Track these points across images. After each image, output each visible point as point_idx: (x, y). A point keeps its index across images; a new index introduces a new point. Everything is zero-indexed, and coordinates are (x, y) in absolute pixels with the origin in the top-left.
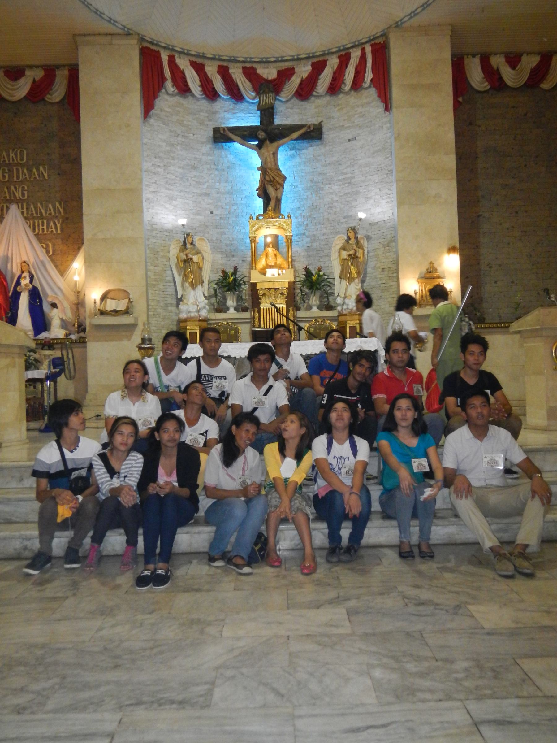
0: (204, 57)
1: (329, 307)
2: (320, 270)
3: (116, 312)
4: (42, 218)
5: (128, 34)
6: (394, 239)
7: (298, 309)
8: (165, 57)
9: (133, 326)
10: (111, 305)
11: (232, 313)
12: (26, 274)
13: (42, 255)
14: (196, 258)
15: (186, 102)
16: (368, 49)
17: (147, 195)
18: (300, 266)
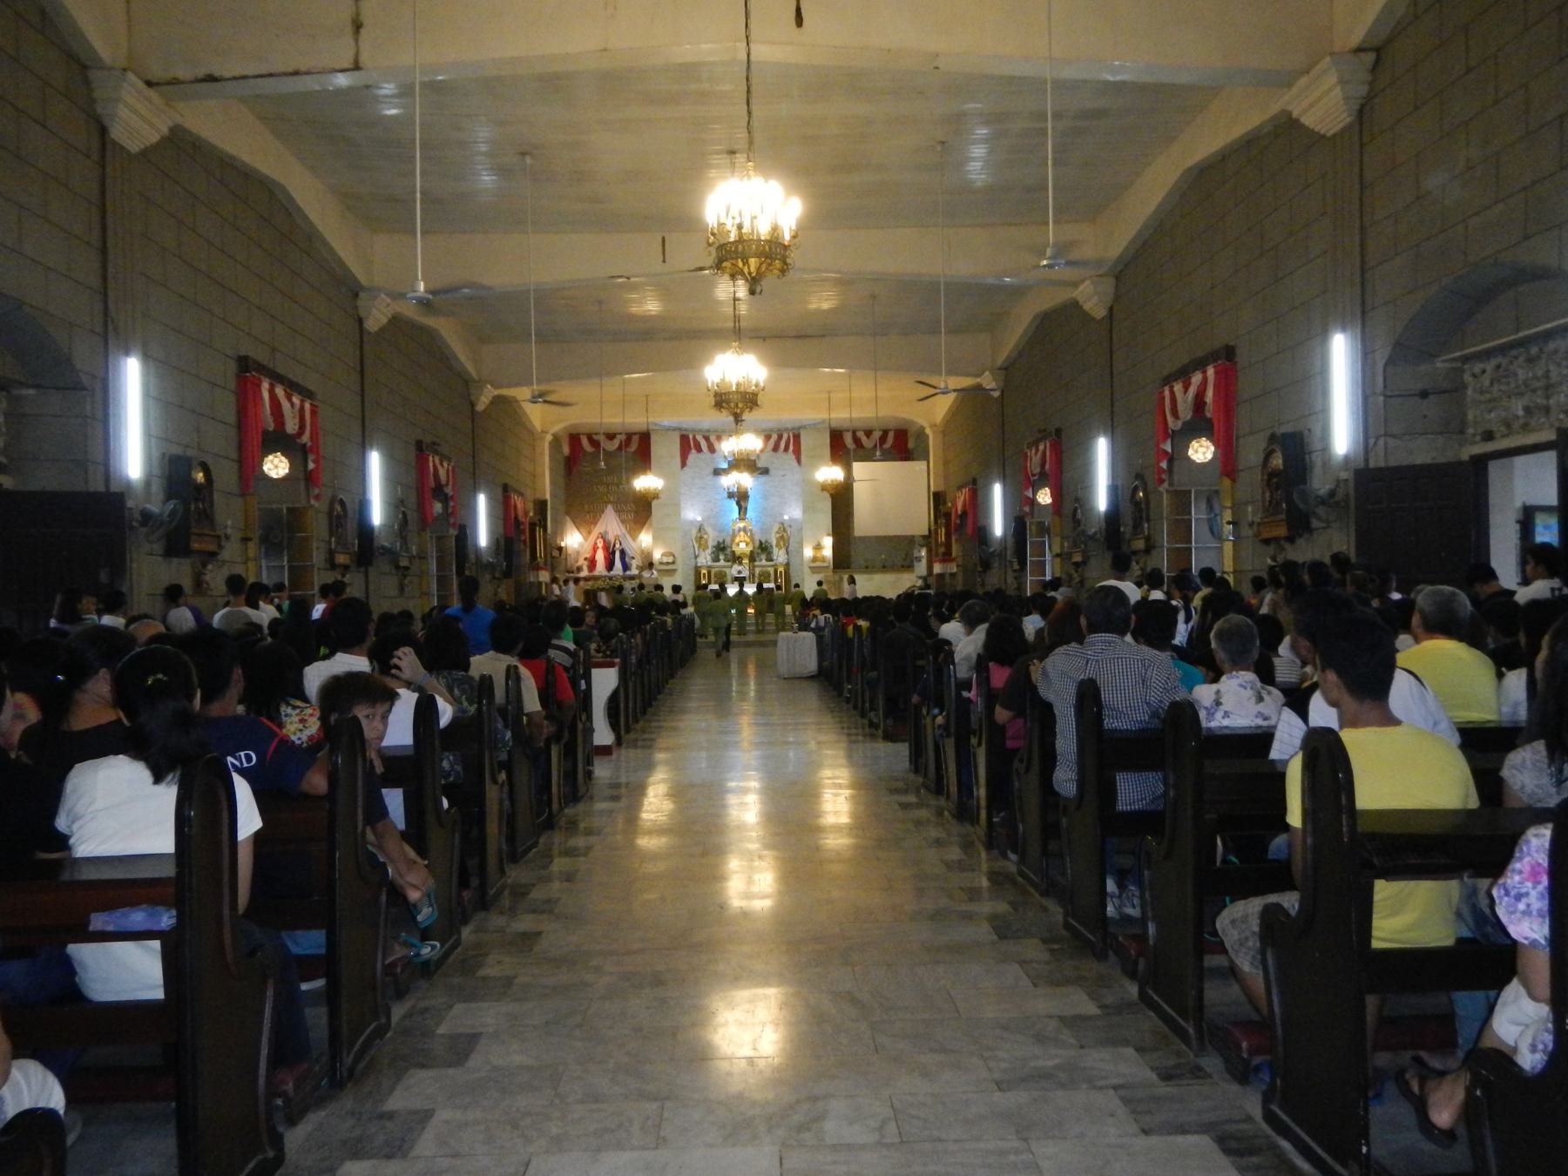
0: (709, 431)
1: (772, 560)
2: (766, 542)
3: (668, 563)
4: (624, 511)
5: (675, 429)
6: (802, 529)
7: (755, 561)
8: (691, 437)
9: (675, 570)
10: (665, 560)
11: (722, 562)
12: (617, 541)
13: (624, 531)
14: (705, 536)
15: (701, 456)
16: (791, 435)
17: (683, 505)
18: (757, 537)
